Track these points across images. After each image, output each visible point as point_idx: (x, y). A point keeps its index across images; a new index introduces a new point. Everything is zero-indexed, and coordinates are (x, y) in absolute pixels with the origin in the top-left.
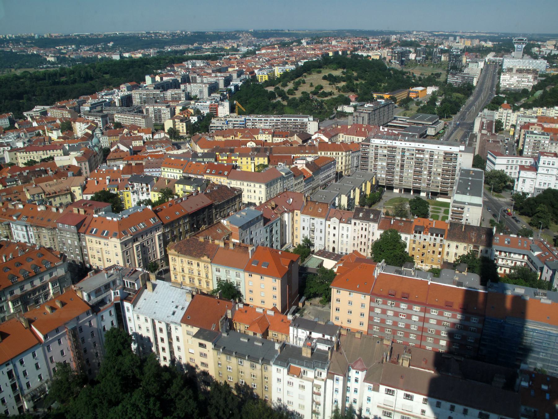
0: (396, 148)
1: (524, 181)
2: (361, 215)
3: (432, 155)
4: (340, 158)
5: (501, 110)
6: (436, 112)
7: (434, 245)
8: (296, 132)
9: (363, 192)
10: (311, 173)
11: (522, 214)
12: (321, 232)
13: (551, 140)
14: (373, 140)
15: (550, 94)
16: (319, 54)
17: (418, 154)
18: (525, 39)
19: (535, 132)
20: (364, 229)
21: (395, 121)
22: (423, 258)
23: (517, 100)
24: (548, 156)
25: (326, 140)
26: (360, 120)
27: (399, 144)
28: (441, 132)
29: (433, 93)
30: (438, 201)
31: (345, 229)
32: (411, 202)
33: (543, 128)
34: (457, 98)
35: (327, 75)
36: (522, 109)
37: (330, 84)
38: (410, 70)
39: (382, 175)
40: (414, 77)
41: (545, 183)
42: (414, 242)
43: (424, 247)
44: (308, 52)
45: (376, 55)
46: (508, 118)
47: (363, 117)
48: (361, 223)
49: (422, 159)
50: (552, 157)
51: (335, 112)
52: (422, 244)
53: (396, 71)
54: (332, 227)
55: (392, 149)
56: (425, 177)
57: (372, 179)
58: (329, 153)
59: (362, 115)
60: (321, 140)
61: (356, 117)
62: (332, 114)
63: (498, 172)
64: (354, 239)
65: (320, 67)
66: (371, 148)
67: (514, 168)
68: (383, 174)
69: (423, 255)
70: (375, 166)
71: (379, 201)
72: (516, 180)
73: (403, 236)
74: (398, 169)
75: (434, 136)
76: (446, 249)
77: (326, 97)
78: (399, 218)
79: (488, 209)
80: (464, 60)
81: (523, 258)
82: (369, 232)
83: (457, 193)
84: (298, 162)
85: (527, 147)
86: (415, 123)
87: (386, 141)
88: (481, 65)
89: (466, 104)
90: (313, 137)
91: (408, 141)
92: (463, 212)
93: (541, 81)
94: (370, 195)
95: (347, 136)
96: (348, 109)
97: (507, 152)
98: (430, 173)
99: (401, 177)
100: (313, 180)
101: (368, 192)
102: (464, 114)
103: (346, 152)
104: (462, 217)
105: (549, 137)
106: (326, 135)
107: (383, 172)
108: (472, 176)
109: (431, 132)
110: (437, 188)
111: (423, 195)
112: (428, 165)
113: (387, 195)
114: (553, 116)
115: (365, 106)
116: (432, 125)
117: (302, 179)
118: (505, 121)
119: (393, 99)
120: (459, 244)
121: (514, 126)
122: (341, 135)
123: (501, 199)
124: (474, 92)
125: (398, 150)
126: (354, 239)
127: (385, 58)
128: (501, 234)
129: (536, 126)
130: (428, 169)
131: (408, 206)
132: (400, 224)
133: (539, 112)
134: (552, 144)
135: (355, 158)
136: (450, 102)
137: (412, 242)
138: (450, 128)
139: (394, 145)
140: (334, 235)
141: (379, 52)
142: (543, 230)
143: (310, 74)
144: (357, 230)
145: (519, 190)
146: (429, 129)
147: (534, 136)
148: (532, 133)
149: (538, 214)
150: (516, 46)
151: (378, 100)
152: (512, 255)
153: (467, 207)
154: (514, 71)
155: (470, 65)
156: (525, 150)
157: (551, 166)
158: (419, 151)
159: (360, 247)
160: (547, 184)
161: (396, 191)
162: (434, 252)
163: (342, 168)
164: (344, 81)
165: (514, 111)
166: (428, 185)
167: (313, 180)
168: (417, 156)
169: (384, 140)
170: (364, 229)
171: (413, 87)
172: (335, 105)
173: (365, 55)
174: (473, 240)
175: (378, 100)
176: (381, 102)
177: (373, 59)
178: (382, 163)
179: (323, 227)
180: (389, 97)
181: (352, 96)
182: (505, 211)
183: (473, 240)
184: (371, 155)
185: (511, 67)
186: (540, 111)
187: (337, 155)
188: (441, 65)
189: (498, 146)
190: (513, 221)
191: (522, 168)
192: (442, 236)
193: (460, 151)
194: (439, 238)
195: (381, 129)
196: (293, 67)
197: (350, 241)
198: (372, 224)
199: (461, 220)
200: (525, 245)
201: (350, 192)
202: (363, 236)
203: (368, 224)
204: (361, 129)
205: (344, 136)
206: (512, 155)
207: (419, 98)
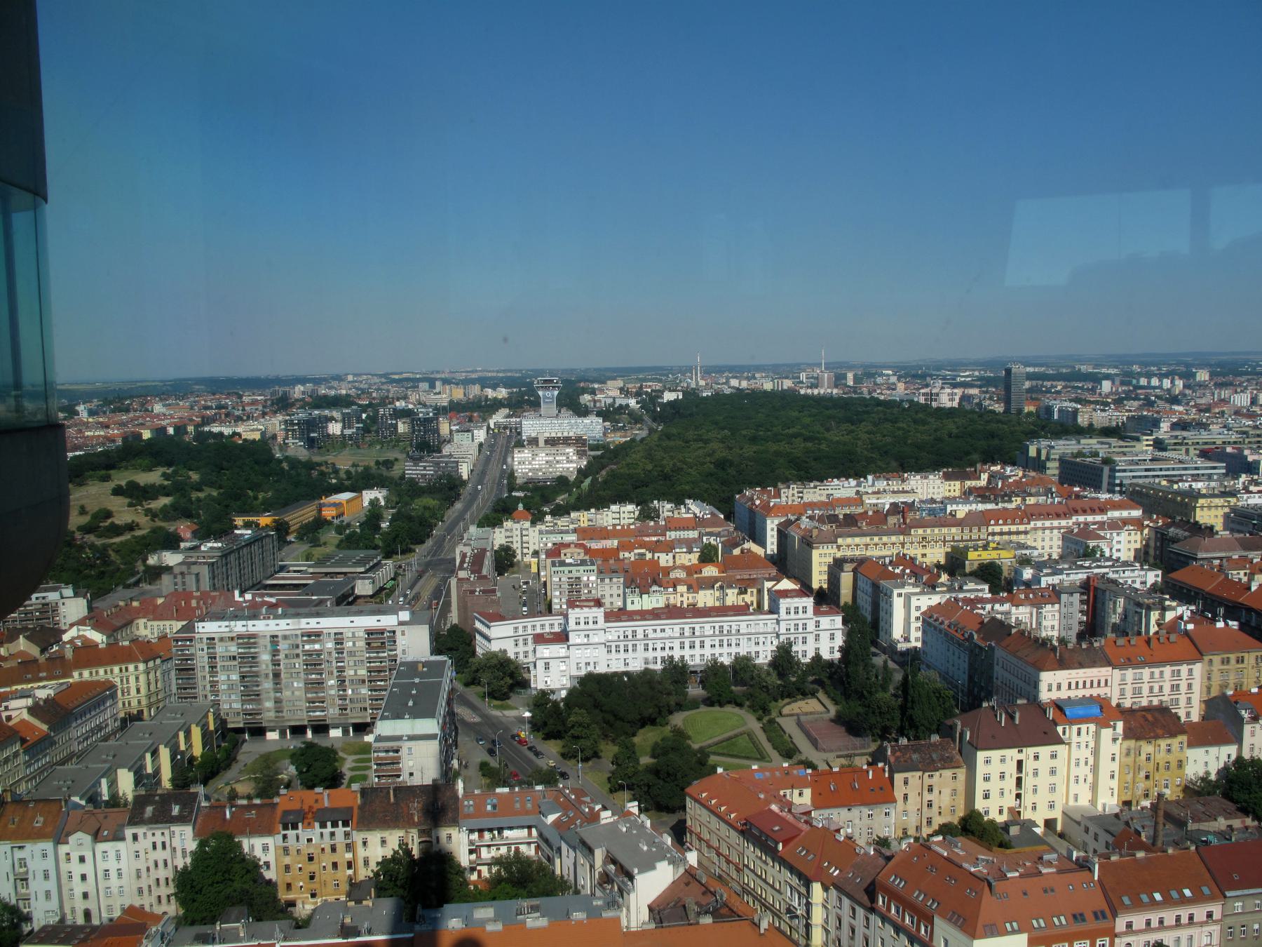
0: (253, 636)
1: (547, 666)
3: (339, 641)
4: (132, 679)
5: (508, 524)
7: (333, 849)
8: (25, 629)
9: (182, 753)
10: (45, 727)
11: (548, 737)
13: (600, 572)
14: (201, 624)
15: (605, 482)
16: (117, 435)
17: (309, 642)
18: (555, 379)
19: (568, 561)
20: (159, 846)
21: (281, 575)
23: (546, 500)
24: (581, 607)
25: (97, 637)
26: (190, 581)
27: (263, 627)
28: (388, 586)
29: (374, 503)
31: (112, 854)
32: (296, 757)
33: (588, 551)
34: (426, 508)
35: (123, 483)
36: (548, 518)
37: (130, 505)
38: (330, 458)
39: (232, 705)
40: (336, 471)
41: (588, 664)
42: (286, 851)
43: (311, 859)
45: (253, 430)
46: (525, 539)
47: (197, 575)
48: (149, 834)
49: (319, 653)
50: (590, 607)
51: (141, 568)
52: (306, 850)
53: (294, 463)
54: (75, 857)
55: (249, 640)
56: (333, 692)
57: (206, 716)
58: (101, 671)
59: (195, 569)
60: (86, 640)
61: (179, 577)
62: (133, 575)
64: (139, 877)
65: (111, 466)
66: (199, 646)
67: (521, 643)
68: (235, 701)
69: (312, 878)
70: (214, 684)
71: (228, 767)
72: (532, 668)
73: (246, 844)
74: (267, 685)
75: (371, 597)
76: (361, 853)
77: (118, 535)
79: (477, 741)
80: (445, 427)
81: (530, 834)
82: (174, 849)
83: (383, 718)
85: (557, 593)
86: (326, 574)
87: (233, 623)
88: (481, 435)
89: (445, 519)
90: (66, 637)
91: (284, 616)
92: (399, 758)
93: (594, 457)
94: (201, 757)
95: (155, 623)
96: (171, 559)
97: (525, 609)
98: (342, 682)
99: (278, 701)
100: (53, 743)
101: (198, 750)
102: (440, 544)
103: (146, 662)
104: (400, 770)
105: (595, 568)
106: (96, 627)
107: (233, 697)
108: (422, 675)
109: (364, 588)
110: (363, 713)
111: (335, 733)
112: (334, 664)
113: (250, 750)
114: (605, 524)
115: (203, 548)
117: (17, 747)
119: (281, 529)
120: (386, 834)
121: (536, 554)
122: (141, 622)
123: (507, 713)
124: (465, 492)
125: (261, 642)
126: (139, 877)
127: (274, 437)
129: (572, 549)
130: (336, 674)
133: (582, 519)
134: (603, 580)
135: (173, 673)
136: (410, 518)
137: (281, 851)
138: (409, 576)
140: (84, 877)
141: (256, 425)
142: (590, 763)
143: (80, 485)
144: (142, 854)
145: (541, 686)
146: (359, 584)
147: (566, 569)
148: (563, 564)
149: (572, 731)
150: (540, 393)
152: (506, 833)
153: (406, 746)
154: (541, 443)
155: (457, 437)
156: (555, 601)
157: (591, 626)
158: (309, 636)
159: (155, 892)
160: (592, 664)
161: (272, 736)
162: (335, 865)
164: (167, 495)
165: (533, 523)
166: (343, 709)
167: (53, 743)
168: (307, 647)
169: (227, 623)
170: (159, 846)
172: (140, 553)
173: (227, 431)
174: (416, 819)
176: (242, 535)
177: (245, 440)
178: (229, 677)
179: (49, 864)
180: (275, 521)
181: (184, 528)
182: (513, 737)
183: (416, 819)
184: (201, 660)
185: (533, 435)
186: (583, 518)
187: (124, 674)
188: (398, 441)
189: (493, 602)
190: (531, 755)
191: (540, 639)
192: (346, 824)
193: (401, 623)
194: (340, 830)
197: (129, 882)
198: (177, 829)
199: (399, 776)
200: (529, 805)
201: (143, 757)
202: (161, 864)
203: (166, 832)
204: (188, 603)
205: (149, 624)
207: (345, 516)
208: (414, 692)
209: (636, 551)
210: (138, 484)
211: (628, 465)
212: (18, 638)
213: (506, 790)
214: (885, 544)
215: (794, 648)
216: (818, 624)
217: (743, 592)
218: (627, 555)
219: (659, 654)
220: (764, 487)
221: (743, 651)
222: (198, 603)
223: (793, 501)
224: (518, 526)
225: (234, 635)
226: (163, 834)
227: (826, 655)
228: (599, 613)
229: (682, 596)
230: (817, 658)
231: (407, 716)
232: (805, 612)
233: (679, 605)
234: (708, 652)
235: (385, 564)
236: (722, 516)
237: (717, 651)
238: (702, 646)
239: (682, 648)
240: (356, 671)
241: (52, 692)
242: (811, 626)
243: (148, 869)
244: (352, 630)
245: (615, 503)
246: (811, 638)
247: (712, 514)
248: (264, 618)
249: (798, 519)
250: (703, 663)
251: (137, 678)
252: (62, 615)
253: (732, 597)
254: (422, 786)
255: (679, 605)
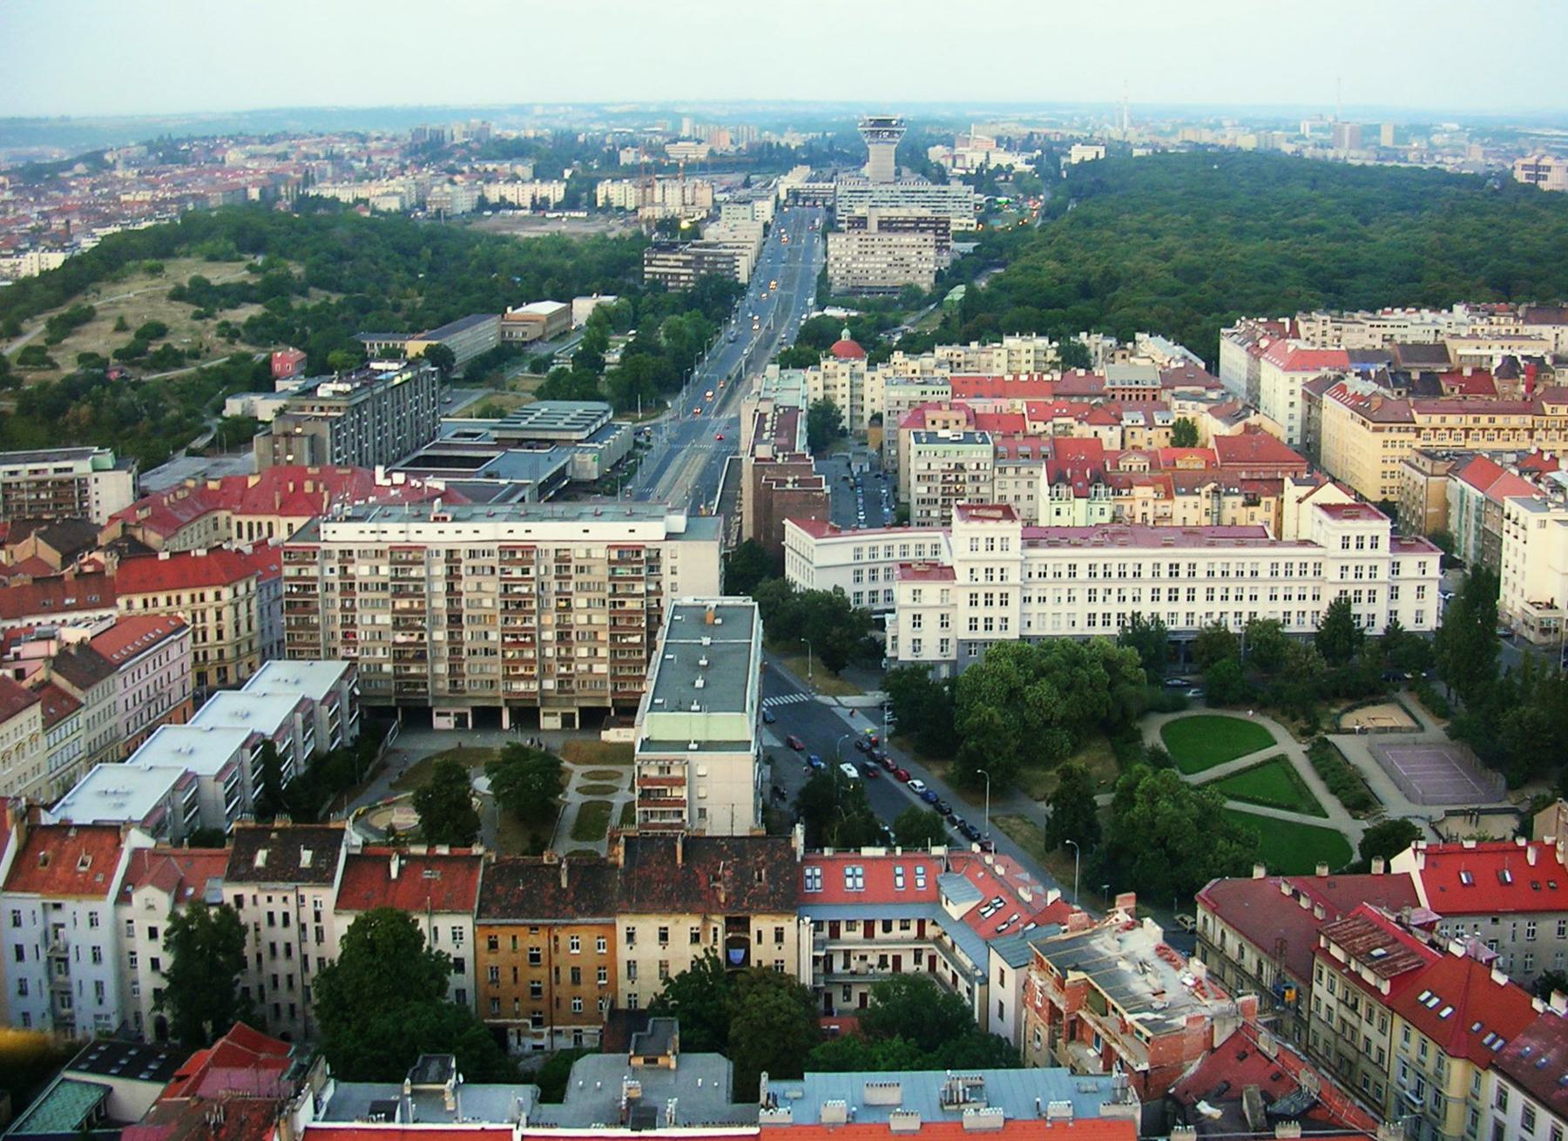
0: (421, 549)
2: (260, 858)
5: (828, 364)
6: (605, 390)
8: (39, 521)
12: (97, 957)
19: (942, 434)
20: (279, 919)
22: (539, 1005)
23: (882, 326)
27: (429, 534)
30: (605, 743)
33: (975, 418)
36: (898, 357)
44: (124, 198)
45: (387, 194)
46: (857, 391)
50: (998, 519)
55: (405, 557)
61: (282, 441)
63: (826, 598)
77: (180, 366)
78: (422, 850)
83: (653, 707)
84: (29, 650)
88: (765, 209)
96: (265, 408)
98: (563, 637)
115: (320, 392)
116: (587, 440)
118: (847, 401)
120: (667, 922)
128: (828, 852)
131: (482, 783)
132: (427, 874)
139: (416, 539)
145: (905, 654)
148: (933, 438)
151: (375, 366)
154: (873, 225)
163: (221, 652)
165: (872, 364)
169: (373, 526)
170: (279, 919)
171: (520, 306)
173: (345, 195)
175: (375, 366)
176: (381, 372)
195: (380, 479)
196: (56, 260)
204: (299, 487)
205: (235, 520)
206: (875, 522)
208: (703, 662)
209: (1058, 421)
210: (207, 282)
211: (1024, 269)
212: (29, 535)
213: (881, 852)
214: (1499, 430)
215: (1355, 609)
216: (1395, 568)
217: (1252, 502)
218: (1041, 427)
219: (1114, 608)
220: (1272, 318)
221: (1266, 610)
222: (316, 488)
223: (1324, 344)
224: (845, 368)
225: (385, 547)
226: (285, 899)
227: (1407, 623)
228: (1013, 530)
229: (1145, 504)
230: (1394, 629)
231: (695, 707)
232: (1374, 546)
233: (1138, 520)
234: (1200, 607)
235: (619, 427)
236: (1202, 365)
237: (1217, 607)
238: (1191, 598)
239: (1155, 599)
240: (589, 618)
241: (87, 633)
242: (1384, 573)
243: (259, 957)
244: (589, 545)
245: (1011, 334)
246: (1383, 595)
247: (1185, 358)
248: (436, 519)
249: (1340, 378)
250: (1190, 628)
251: (219, 616)
252: (94, 498)
253: (1234, 508)
254: (732, 837)
255: (1138, 520)
